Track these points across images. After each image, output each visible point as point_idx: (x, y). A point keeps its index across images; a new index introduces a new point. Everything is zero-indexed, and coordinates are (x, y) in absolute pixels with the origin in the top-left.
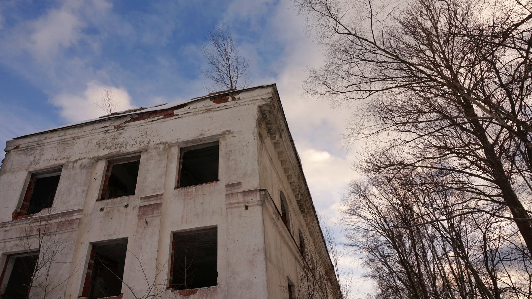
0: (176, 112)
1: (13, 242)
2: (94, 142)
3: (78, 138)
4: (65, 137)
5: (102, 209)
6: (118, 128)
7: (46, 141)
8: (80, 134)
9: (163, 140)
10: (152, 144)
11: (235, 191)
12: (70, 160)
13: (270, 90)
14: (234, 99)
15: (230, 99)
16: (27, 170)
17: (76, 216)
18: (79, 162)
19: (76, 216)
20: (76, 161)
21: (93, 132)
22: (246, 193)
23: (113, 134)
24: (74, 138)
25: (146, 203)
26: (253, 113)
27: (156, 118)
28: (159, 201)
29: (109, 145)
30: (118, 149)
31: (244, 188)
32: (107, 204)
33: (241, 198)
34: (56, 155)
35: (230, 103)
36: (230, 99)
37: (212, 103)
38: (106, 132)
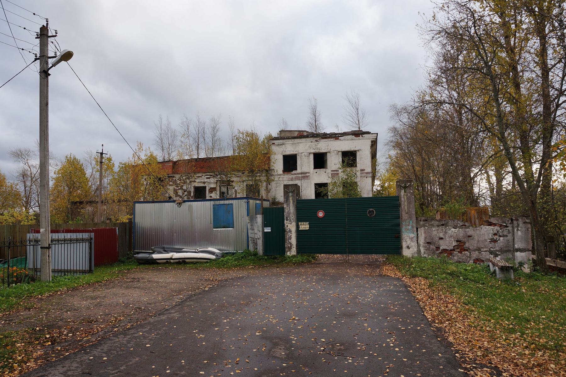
0: (340, 138)
1: (286, 182)
2: (308, 145)
3: (300, 143)
4: (295, 142)
5: (316, 172)
6: (317, 141)
7: (286, 143)
9: (336, 149)
10: (332, 150)
11: (363, 172)
12: (299, 152)
13: (376, 135)
14: (362, 136)
15: (361, 136)
16: (282, 154)
17: (308, 175)
18: (303, 154)
19: (308, 175)
20: (302, 153)
22: (367, 173)
24: (298, 143)
25: (333, 173)
26: (369, 143)
27: (332, 139)
28: (337, 172)
29: (315, 148)
30: (318, 150)
31: (366, 171)
33: (365, 175)
34: (293, 149)
35: (361, 137)
36: (361, 136)
37: (354, 137)
38: (312, 142)
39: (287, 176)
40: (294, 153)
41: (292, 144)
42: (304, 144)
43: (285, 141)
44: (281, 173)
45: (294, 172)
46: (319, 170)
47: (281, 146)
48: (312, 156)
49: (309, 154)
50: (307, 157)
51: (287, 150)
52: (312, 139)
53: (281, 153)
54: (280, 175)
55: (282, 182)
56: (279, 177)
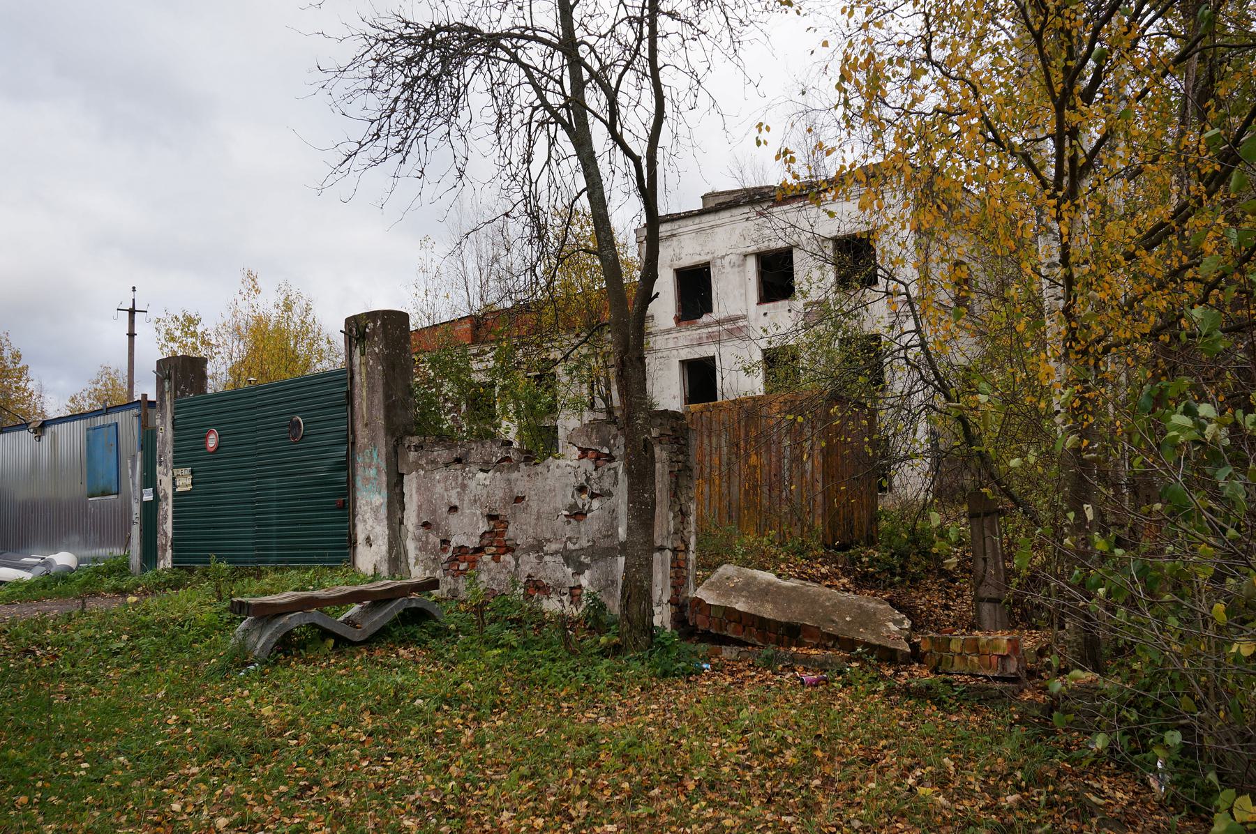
2: (737, 232)
3: (717, 226)
4: (702, 226)
5: (765, 314)
8: (719, 222)
16: (671, 267)
20: (723, 257)
21: (732, 219)
23: (756, 222)
24: (712, 227)
30: (766, 244)
32: (769, 309)
34: (698, 249)
38: (747, 219)
39: (688, 333)
40: (704, 258)
41: (698, 231)
42: (728, 228)
43: (675, 225)
44: (672, 324)
45: (705, 318)
46: (771, 305)
47: (668, 243)
48: (752, 264)
49: (742, 257)
50: (736, 269)
51: (684, 252)
52: (746, 209)
53: (669, 262)
54: (669, 331)
55: (675, 352)
56: (667, 336)
